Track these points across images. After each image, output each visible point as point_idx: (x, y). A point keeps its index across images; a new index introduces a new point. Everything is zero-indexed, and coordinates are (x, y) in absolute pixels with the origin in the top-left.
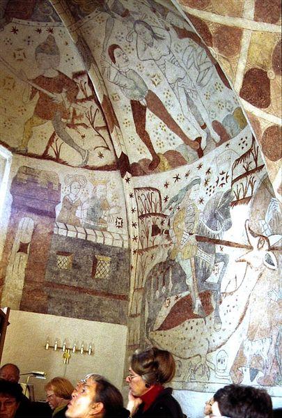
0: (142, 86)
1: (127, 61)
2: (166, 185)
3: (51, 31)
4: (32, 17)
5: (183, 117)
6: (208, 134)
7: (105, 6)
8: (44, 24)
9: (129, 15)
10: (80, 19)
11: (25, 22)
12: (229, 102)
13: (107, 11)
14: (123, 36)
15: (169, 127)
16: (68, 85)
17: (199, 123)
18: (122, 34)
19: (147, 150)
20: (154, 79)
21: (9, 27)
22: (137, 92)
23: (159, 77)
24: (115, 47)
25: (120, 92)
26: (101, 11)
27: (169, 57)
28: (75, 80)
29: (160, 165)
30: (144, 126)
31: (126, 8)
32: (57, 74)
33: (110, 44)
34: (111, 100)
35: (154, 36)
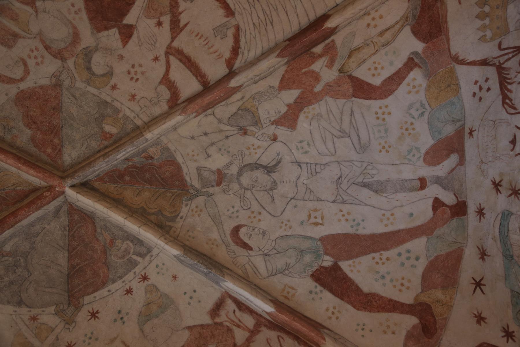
0: (306, 245)
1: (264, 233)
2: (480, 319)
3: (145, 278)
4: (111, 277)
5: (388, 214)
6: (438, 181)
7: (191, 191)
8: (131, 275)
9: (226, 174)
10: (171, 227)
11: (104, 292)
12: (410, 107)
13: (198, 193)
14: (236, 209)
15: (387, 249)
16: (213, 336)
17: (412, 190)
18: (233, 207)
19: (396, 317)
20: (313, 220)
21: (83, 315)
22: (308, 258)
23: (316, 210)
24: (236, 230)
25: (287, 280)
26: (190, 199)
27: (305, 173)
28: (218, 320)
29: (437, 309)
30: (358, 289)
31: (214, 169)
32: (187, 333)
33: (228, 232)
34: (286, 302)
35: (269, 170)
